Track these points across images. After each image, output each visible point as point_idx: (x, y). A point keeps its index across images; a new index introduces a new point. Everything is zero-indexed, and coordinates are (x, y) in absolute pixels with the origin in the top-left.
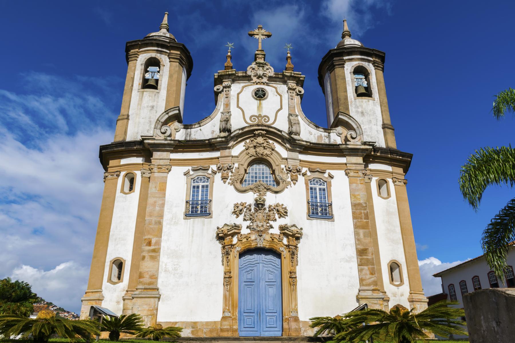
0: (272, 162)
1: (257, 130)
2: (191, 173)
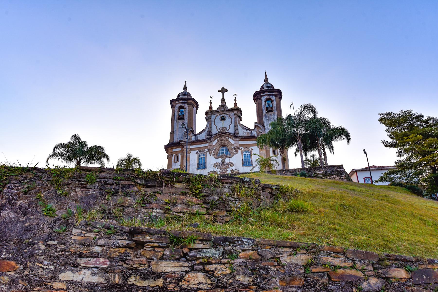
2: (199, 152)
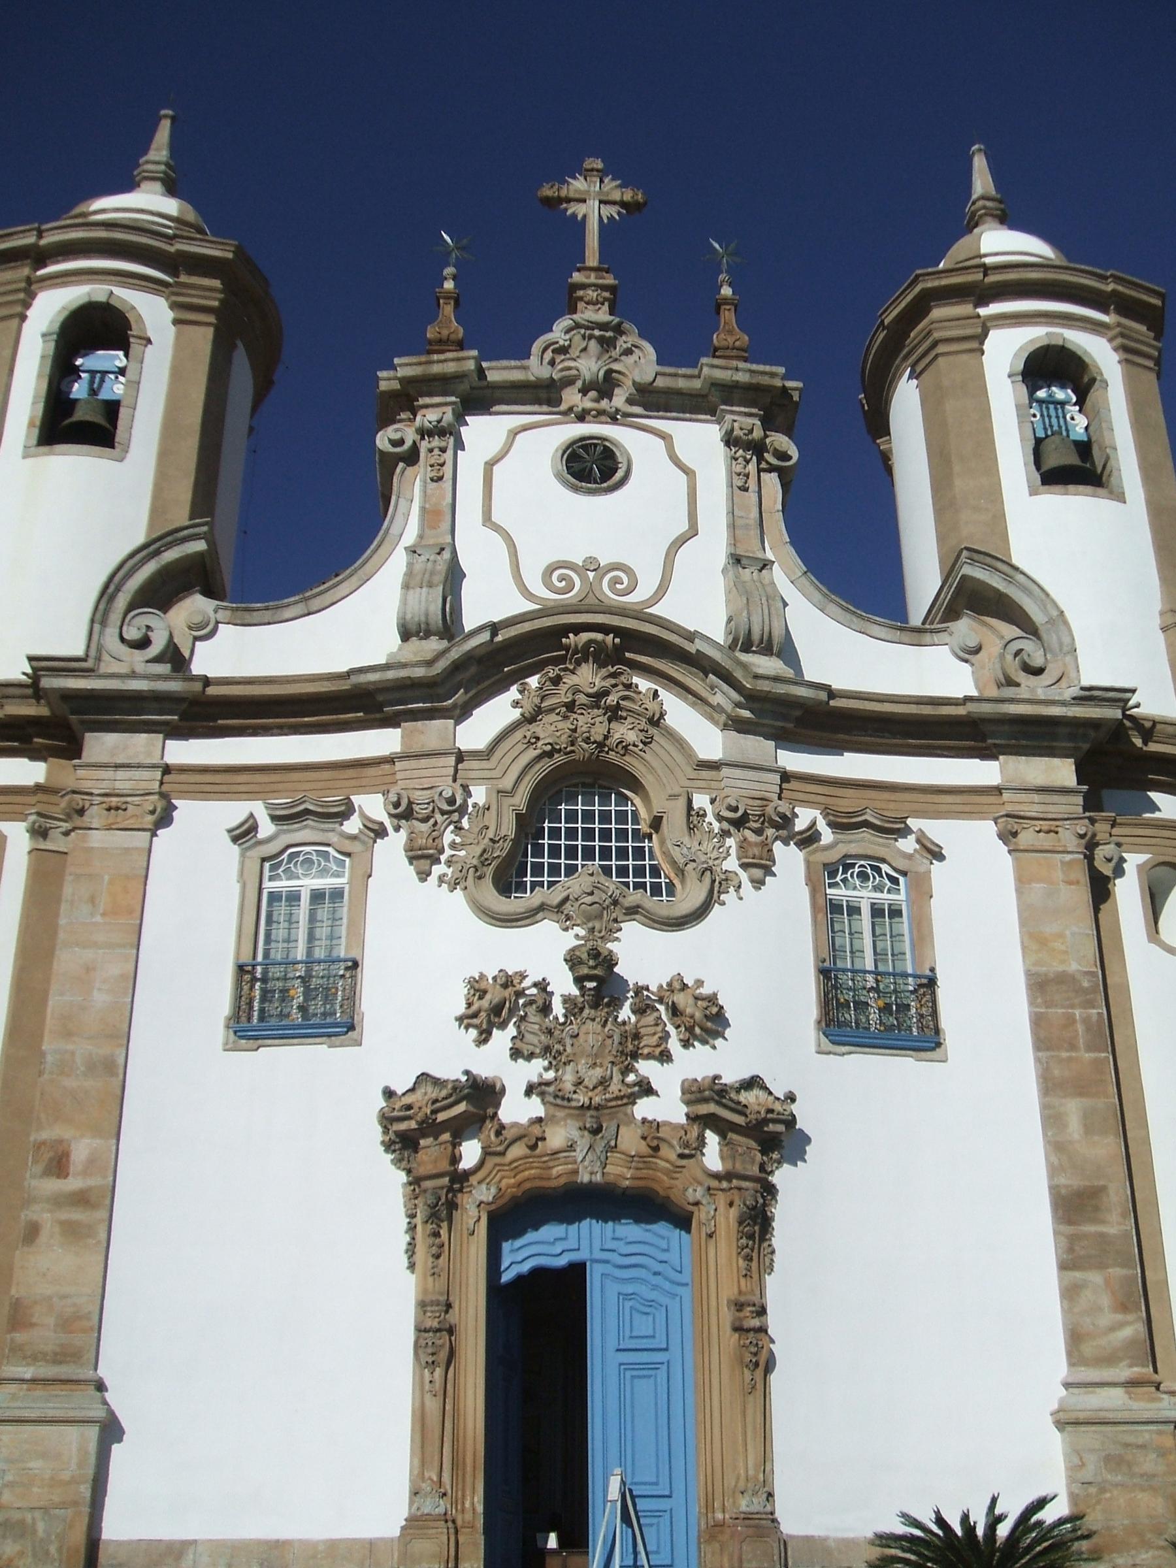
0: (647, 780)
1: (578, 629)
2: (266, 828)
